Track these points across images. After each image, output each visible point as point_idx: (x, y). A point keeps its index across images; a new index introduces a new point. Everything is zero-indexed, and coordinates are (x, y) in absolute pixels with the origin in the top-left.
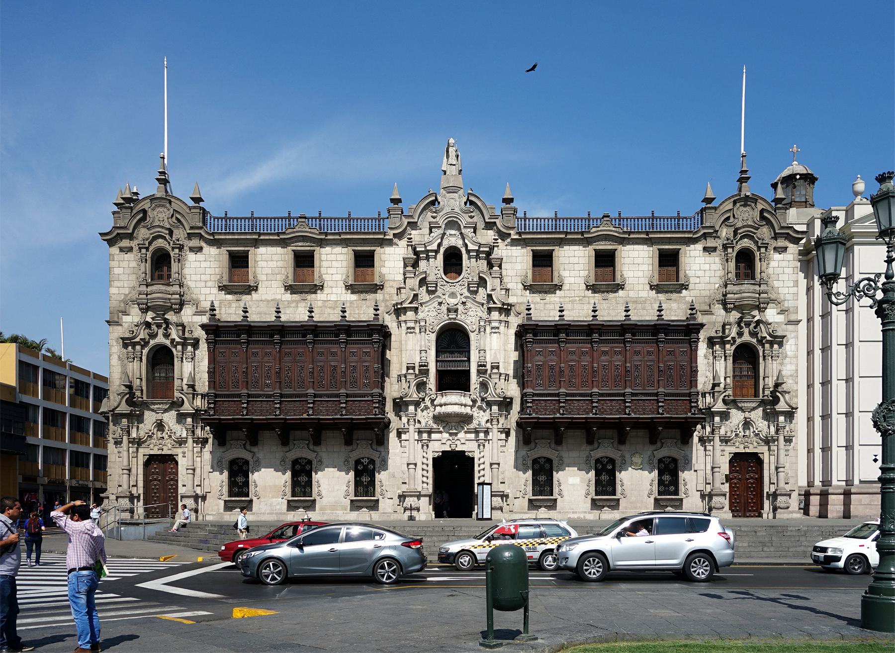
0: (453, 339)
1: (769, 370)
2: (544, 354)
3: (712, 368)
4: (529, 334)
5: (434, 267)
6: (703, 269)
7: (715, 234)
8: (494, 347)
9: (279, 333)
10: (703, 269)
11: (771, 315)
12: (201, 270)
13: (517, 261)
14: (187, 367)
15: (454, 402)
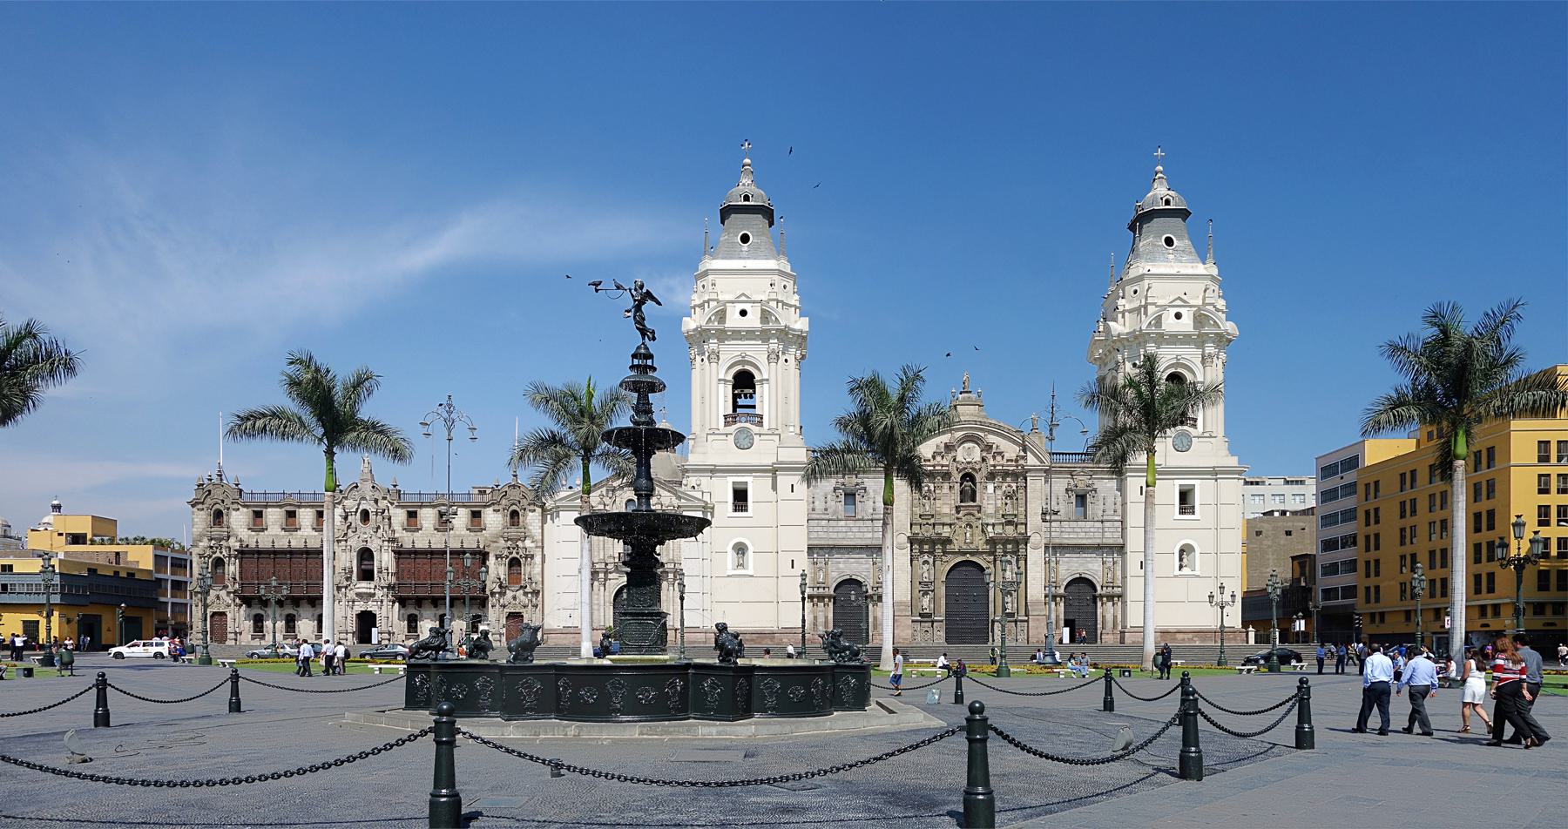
0: (366, 555)
1: (525, 570)
2: (408, 563)
3: (496, 570)
4: (400, 554)
5: (355, 519)
6: (493, 520)
7: (499, 503)
8: (385, 559)
9: (275, 553)
10: (493, 520)
11: (528, 543)
12: (239, 520)
13: (399, 516)
14: (232, 568)
15: (364, 587)
